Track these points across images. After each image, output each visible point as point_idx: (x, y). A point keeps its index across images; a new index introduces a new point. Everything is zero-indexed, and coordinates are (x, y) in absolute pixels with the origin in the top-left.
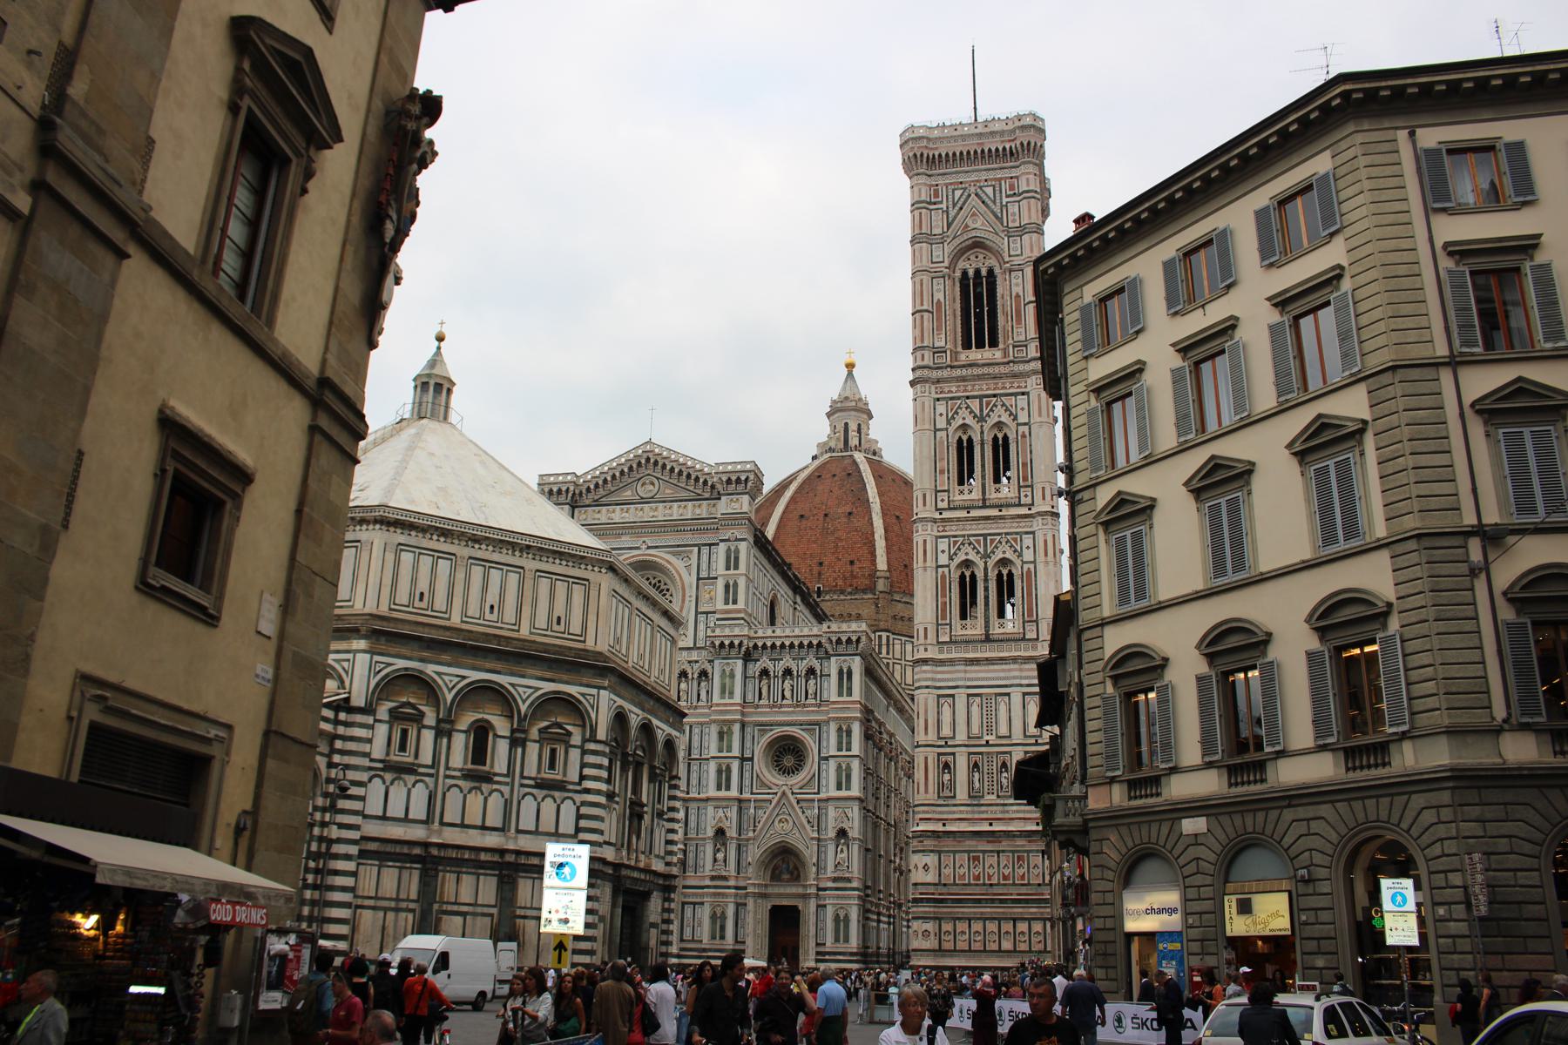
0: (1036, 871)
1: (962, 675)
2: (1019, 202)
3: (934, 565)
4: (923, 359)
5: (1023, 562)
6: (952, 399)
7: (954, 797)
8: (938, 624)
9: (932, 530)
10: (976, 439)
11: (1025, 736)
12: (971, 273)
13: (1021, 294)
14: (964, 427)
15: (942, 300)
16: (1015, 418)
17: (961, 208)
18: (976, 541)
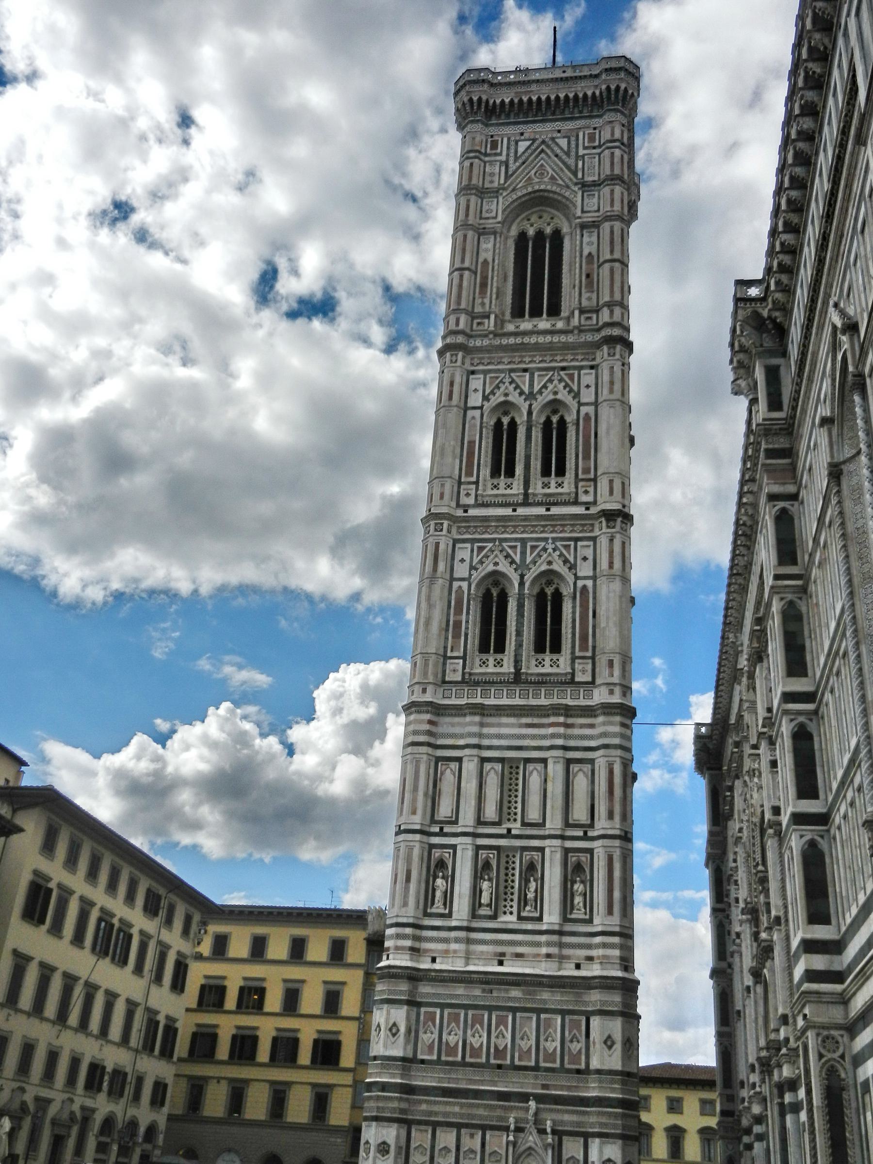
0: (575, 1047)
1: (475, 729)
2: (599, 154)
3: (448, 576)
4: (457, 324)
5: (577, 578)
6: (490, 371)
7: (450, 915)
8: (445, 657)
9: (449, 531)
10: (521, 419)
11: (567, 825)
12: (531, 232)
13: (594, 253)
14: (506, 407)
15: (490, 260)
16: (577, 395)
17: (524, 163)
18: (511, 547)
